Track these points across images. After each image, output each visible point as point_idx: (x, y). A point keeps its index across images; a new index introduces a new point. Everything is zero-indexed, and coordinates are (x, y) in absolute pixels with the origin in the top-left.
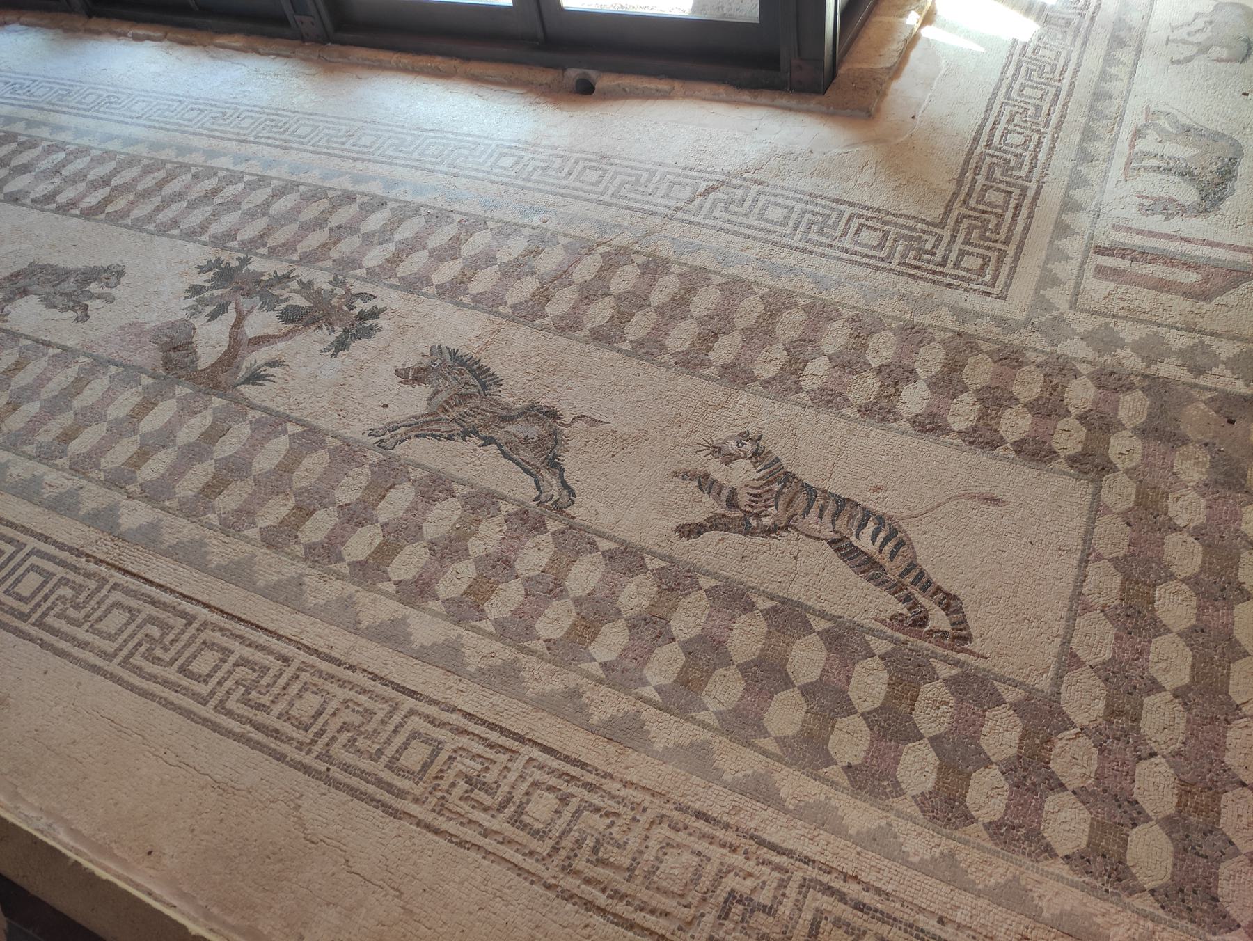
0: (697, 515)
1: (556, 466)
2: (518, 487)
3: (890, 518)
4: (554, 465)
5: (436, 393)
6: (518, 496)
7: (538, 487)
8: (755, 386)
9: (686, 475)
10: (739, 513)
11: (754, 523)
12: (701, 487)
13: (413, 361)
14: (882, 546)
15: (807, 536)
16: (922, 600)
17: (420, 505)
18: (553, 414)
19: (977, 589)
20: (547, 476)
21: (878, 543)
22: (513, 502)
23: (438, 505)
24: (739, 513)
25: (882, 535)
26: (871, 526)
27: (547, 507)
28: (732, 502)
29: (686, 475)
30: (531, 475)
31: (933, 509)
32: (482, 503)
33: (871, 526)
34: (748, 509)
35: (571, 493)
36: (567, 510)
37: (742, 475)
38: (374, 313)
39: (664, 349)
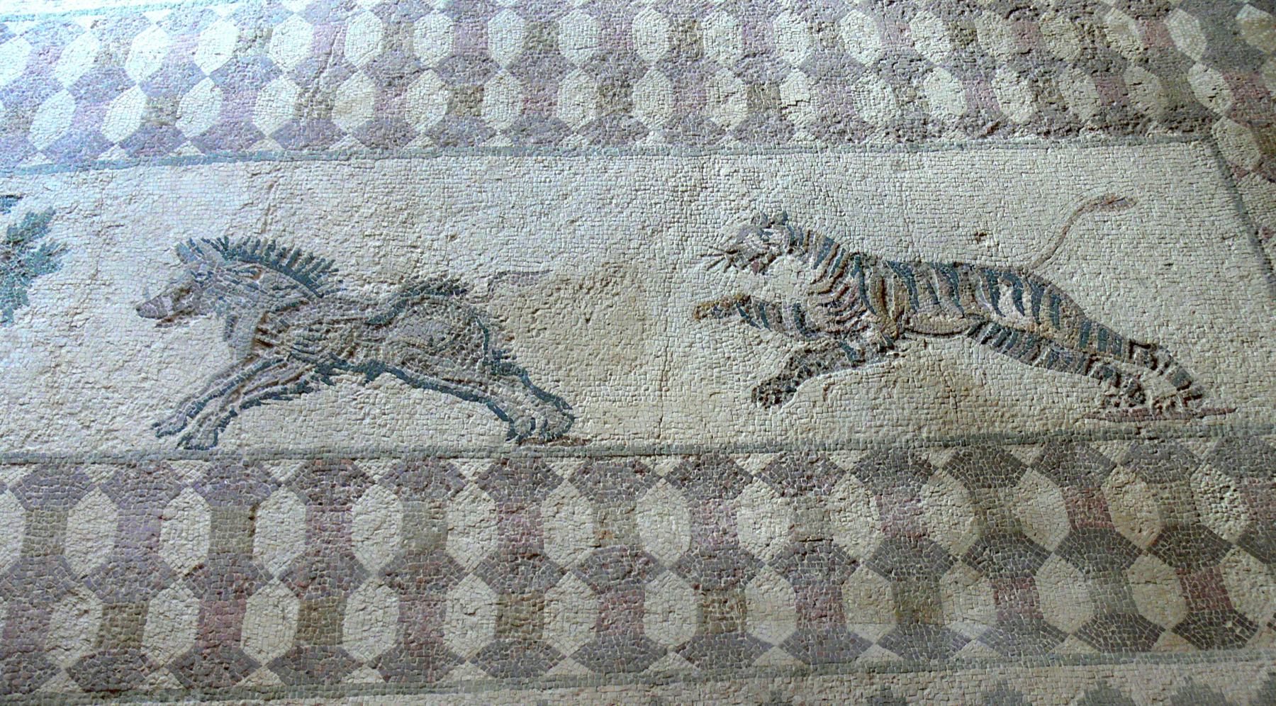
0: (770, 363)
1: (506, 370)
2: (470, 428)
3: (1020, 269)
4: (502, 368)
5: (232, 321)
6: (476, 442)
7: (501, 416)
8: (729, 141)
9: (721, 310)
10: (824, 339)
11: (855, 345)
12: (747, 319)
13: (158, 285)
14: (1036, 311)
15: (935, 335)
16: (1124, 367)
17: (327, 519)
18: (453, 289)
19: (1172, 328)
20: (503, 391)
21: (1028, 312)
22: (477, 453)
23: (356, 508)
24: (824, 339)
25: (1026, 297)
26: (1006, 293)
27: (535, 441)
28: (808, 331)
29: (721, 310)
30: (476, 399)
31: (1061, 239)
32: (424, 473)
33: (1006, 293)
34: (834, 328)
35: (559, 403)
36: (571, 434)
37: (791, 280)
38: (38, 225)
39: (561, 127)
